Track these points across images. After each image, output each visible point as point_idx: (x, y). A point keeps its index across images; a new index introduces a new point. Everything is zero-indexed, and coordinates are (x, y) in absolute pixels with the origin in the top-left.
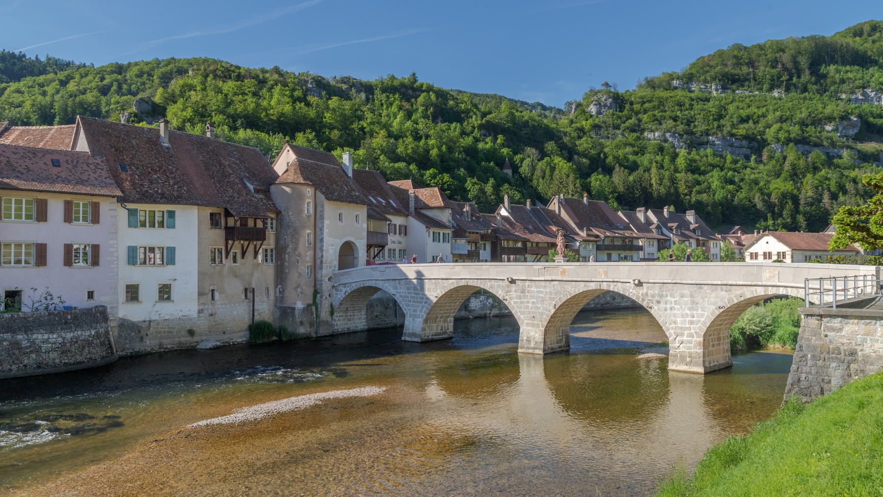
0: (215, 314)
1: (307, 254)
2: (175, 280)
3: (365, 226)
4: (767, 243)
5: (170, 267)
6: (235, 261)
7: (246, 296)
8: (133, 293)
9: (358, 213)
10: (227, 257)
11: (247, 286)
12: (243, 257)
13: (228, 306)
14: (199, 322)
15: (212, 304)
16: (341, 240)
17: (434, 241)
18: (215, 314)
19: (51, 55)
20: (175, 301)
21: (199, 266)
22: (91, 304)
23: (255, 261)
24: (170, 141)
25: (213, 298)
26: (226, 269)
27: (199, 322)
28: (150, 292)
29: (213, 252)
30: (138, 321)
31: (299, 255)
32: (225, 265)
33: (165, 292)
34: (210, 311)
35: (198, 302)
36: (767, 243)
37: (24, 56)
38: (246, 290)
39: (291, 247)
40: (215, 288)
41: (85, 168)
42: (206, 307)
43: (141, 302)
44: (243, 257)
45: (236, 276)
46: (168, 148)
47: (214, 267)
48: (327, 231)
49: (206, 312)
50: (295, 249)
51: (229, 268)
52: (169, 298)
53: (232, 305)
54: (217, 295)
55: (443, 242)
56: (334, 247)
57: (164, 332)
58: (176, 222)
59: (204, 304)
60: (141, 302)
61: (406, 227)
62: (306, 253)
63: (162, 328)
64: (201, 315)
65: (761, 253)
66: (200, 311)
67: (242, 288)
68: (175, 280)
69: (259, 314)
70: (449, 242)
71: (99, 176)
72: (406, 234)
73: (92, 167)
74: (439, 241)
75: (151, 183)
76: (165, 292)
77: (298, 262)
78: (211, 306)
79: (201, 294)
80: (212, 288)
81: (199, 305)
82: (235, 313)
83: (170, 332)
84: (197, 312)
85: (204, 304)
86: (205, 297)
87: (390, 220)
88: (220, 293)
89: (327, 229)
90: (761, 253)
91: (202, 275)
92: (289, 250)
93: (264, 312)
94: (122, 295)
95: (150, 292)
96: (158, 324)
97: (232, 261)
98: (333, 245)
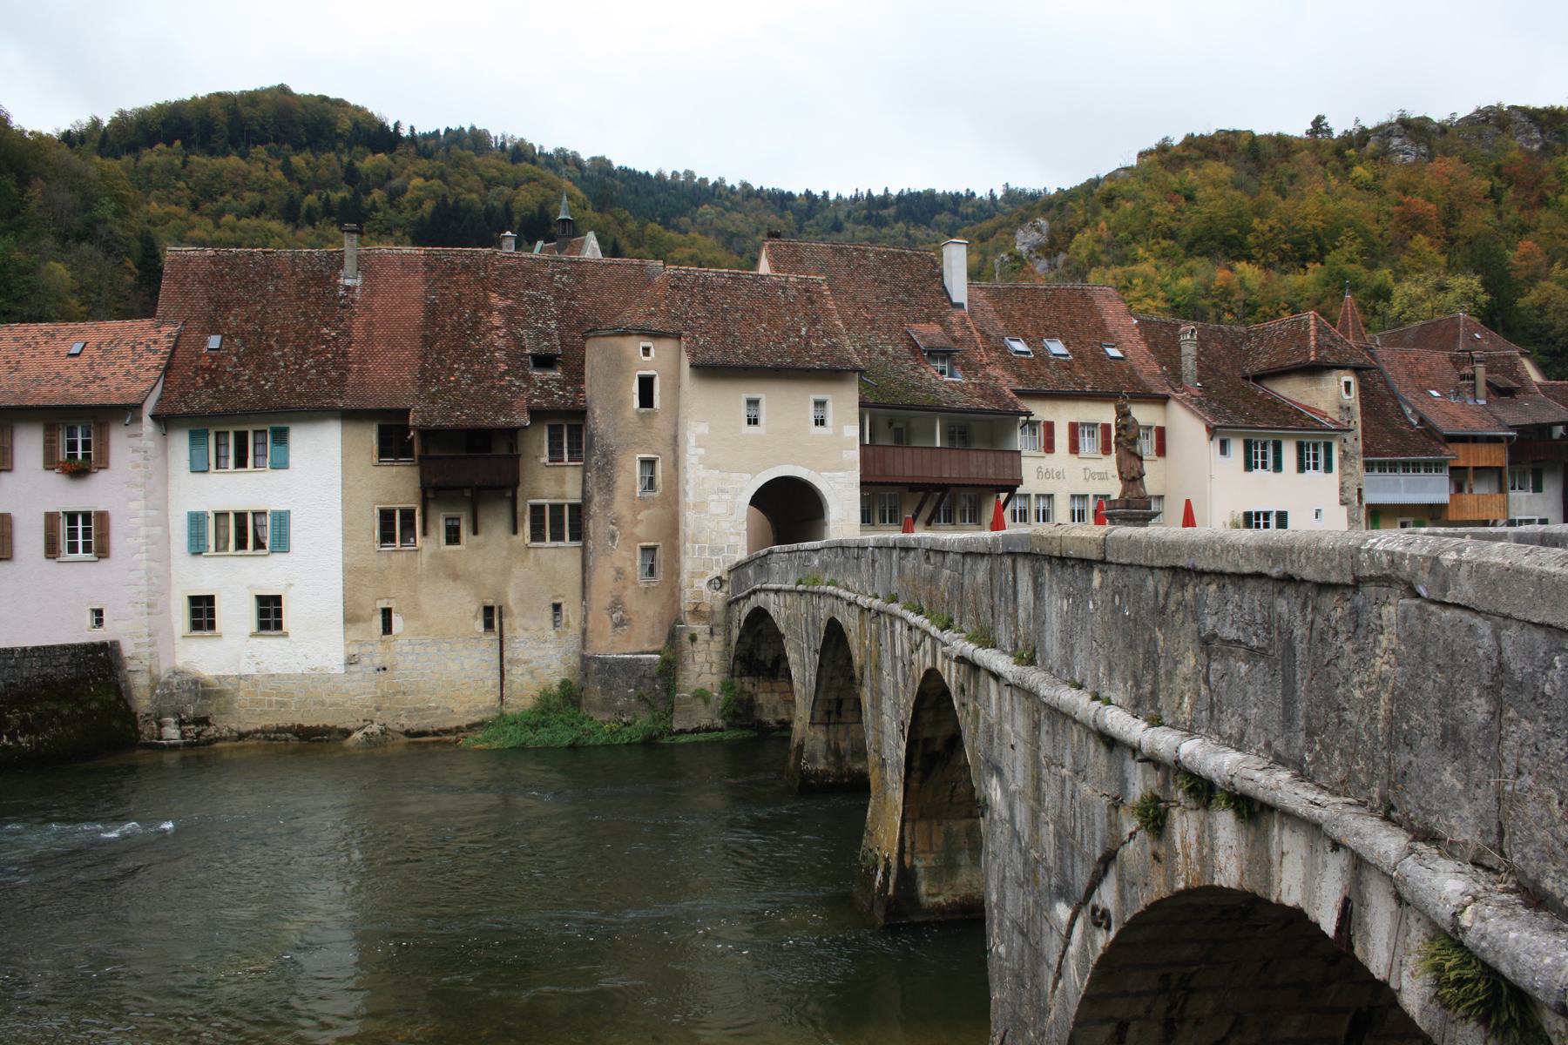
0: (394, 667)
1: (639, 517)
3: (852, 431)
5: (277, 558)
6: (453, 536)
7: (489, 625)
8: (202, 612)
9: (820, 397)
10: (425, 533)
11: (490, 602)
12: (475, 532)
13: (432, 650)
14: (348, 685)
15: (383, 642)
17: (1249, 466)
18: (394, 667)
19: (1012, 186)
21: (345, 554)
22: (98, 636)
23: (515, 538)
25: (387, 628)
26: (423, 559)
27: (348, 685)
28: (235, 613)
29: (386, 516)
30: (218, 678)
31: (615, 521)
33: (270, 612)
34: (378, 661)
35: (345, 639)
37: (973, 194)
38: (488, 611)
39: (597, 499)
40: (392, 605)
44: (475, 532)
45: (455, 577)
48: (701, 451)
49: (366, 661)
50: (607, 505)
51: (433, 556)
53: (446, 646)
54: (397, 622)
55: (1302, 468)
56: (726, 497)
57: (270, 704)
58: (292, 453)
59: (360, 643)
61: (1161, 433)
62: (635, 515)
63: (264, 694)
64: (353, 668)
66: (351, 661)
69: (531, 673)
70: (1328, 469)
74: (1278, 467)
76: (270, 612)
77: (613, 537)
78: (379, 648)
79: (350, 619)
81: (347, 646)
82: (454, 666)
83: (283, 704)
85: (360, 643)
86: (361, 626)
87: (1029, 414)
88: (406, 618)
89: (698, 446)
91: (353, 575)
93: (548, 666)
94: (181, 616)
95: (235, 613)
96: (255, 684)
97: (443, 540)
98: (723, 491)
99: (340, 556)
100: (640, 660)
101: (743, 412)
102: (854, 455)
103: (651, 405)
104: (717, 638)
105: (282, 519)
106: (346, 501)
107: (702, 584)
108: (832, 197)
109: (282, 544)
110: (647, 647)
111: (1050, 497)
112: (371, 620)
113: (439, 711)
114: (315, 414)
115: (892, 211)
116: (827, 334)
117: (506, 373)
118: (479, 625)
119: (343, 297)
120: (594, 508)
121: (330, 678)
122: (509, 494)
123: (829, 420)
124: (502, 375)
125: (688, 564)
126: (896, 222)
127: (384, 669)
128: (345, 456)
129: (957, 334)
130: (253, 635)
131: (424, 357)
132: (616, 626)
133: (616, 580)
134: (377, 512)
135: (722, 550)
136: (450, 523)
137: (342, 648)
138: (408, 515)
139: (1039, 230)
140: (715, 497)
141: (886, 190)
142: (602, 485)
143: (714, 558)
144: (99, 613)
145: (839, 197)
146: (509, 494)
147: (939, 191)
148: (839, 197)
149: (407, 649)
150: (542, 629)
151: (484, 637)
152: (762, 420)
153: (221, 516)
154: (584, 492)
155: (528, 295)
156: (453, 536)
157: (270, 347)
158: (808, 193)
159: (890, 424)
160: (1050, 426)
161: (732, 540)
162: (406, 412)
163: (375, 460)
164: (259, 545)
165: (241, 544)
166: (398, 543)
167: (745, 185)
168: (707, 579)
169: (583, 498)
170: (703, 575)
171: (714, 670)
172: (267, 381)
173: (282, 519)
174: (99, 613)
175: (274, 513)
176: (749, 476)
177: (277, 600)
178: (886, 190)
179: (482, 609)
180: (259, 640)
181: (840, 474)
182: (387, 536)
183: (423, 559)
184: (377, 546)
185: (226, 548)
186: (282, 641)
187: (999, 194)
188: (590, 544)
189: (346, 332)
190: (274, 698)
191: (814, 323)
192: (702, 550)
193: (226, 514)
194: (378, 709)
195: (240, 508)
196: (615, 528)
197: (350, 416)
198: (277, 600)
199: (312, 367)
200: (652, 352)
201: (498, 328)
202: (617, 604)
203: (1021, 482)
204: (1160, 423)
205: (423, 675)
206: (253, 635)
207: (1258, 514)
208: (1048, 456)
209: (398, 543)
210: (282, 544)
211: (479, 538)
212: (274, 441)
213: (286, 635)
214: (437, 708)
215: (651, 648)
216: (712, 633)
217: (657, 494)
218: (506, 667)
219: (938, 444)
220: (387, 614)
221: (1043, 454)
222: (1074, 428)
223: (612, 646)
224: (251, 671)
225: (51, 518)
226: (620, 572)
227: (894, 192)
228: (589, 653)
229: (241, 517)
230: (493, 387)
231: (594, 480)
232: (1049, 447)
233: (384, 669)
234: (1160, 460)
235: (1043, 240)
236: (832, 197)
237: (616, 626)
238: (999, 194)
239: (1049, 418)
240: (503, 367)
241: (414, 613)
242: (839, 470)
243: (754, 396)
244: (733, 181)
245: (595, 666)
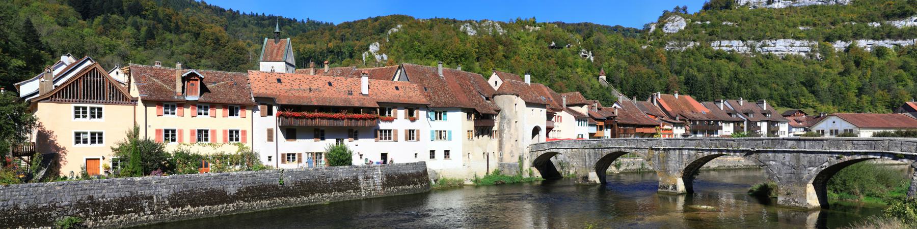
4: (834, 122)
8: (432, 153)
22: (416, 160)
24: (443, 74)
28: (440, 154)
33: (447, 153)
36: (834, 122)
37: (296, 20)
38: (484, 153)
39: (507, 130)
41: (410, 90)
45: (479, 146)
46: (443, 78)
61: (561, 117)
65: (827, 130)
71: (417, 94)
72: (561, 122)
73: (413, 90)
75: (438, 96)
76: (447, 153)
79: (464, 156)
90: (827, 130)
92: (505, 132)
95: (440, 154)
108: (241, 13)
114: (454, 109)
115: (267, 22)
126: (269, 27)
139: (376, 46)
141: (263, 14)
144: (416, 154)
145: (244, 14)
147: (284, 17)
148: (244, 14)
158: (231, 10)
165: (441, 138)
173: (450, 132)
174: (416, 154)
175: (448, 131)
178: (263, 14)
182: (469, 139)
188: (504, 139)
195: (441, 130)
197: (463, 110)
202: (511, 152)
212: (444, 114)
213: (451, 159)
223: (508, 159)
225: (406, 130)
227: (267, 15)
235: (378, 49)
238: (305, 21)
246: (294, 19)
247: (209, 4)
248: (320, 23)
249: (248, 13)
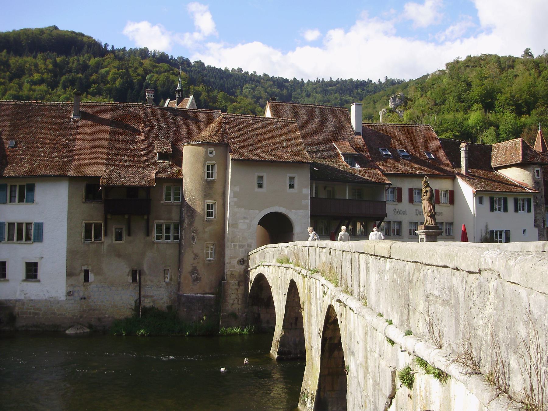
1: (206, 230)
2: (42, 258)
3: (307, 191)
5: (37, 245)
6: (119, 237)
7: (134, 280)
9: (292, 175)
10: (106, 234)
11: (135, 268)
15: (84, 286)
16: (260, 212)
19: (389, 78)
20: (41, 280)
21: (68, 243)
23: (148, 238)
25: (86, 279)
26: (105, 247)
31: (195, 231)
32: (103, 243)
34: (81, 294)
35: (67, 284)
37: (371, 81)
39: (186, 221)
40: (90, 268)
42: (76, 289)
43: (8, 281)
44: (129, 234)
45: (119, 256)
47: (88, 244)
49: (76, 294)
50: (191, 224)
52: (35, 276)
54: (91, 277)
56: (247, 221)
57: (30, 313)
60: (8, 281)
64: (69, 298)
66: (69, 294)
67: (127, 270)
68: (42, 258)
69: (154, 301)
74: (506, 210)
77: (193, 239)
78: (82, 288)
79: (70, 274)
80: (85, 268)
81: (67, 287)
84: (65, 295)
88: (96, 274)
91: (71, 254)
93: (162, 299)
96: (23, 304)
97: (114, 238)
98: (245, 218)
99: (66, 245)
100: (204, 297)
101: (255, 182)
102: (307, 202)
103: (212, 177)
104: (241, 287)
105: (39, 227)
106: (70, 219)
107: (235, 262)
109: (39, 238)
110: (207, 291)
111: (400, 223)
112: (79, 275)
113: (110, 319)
116: (296, 146)
117: (147, 161)
118: (130, 279)
119: (72, 124)
120: (185, 225)
121: (58, 302)
122: (146, 217)
123: (296, 186)
124: (145, 162)
125: (228, 253)
126: (335, 93)
127: (85, 298)
128: (70, 197)
129: (358, 147)
130: (23, 281)
131: (108, 153)
132: (194, 281)
133: (194, 259)
134: (83, 224)
135: (244, 246)
136: (117, 230)
137: (65, 288)
138: (98, 227)
140: (242, 221)
142: (189, 214)
143: (241, 249)
145: (309, 81)
146: (146, 217)
147: (355, 79)
148: (309, 81)
149: (96, 289)
150: (159, 281)
151: (132, 285)
152: (265, 185)
153: (11, 225)
154: (180, 217)
155: (157, 125)
156: (119, 237)
157: (38, 147)
158: (295, 79)
159: (325, 189)
160: (400, 190)
161: (249, 241)
162: (99, 178)
163: (84, 200)
164: (28, 238)
165: (20, 238)
166: (93, 239)
167: (266, 75)
168: (237, 259)
169: (180, 221)
170: (235, 258)
171: (240, 303)
172: (36, 162)
173: (39, 227)
176: (258, 211)
177: (35, 264)
179: (131, 271)
180: (25, 283)
181: (301, 211)
182: (88, 236)
183: (105, 247)
184: (83, 240)
185: (13, 240)
186: (37, 284)
187: (383, 81)
188: (183, 242)
189: (73, 141)
190: (32, 311)
191: (289, 141)
192: (235, 246)
193: (13, 224)
194: (81, 317)
196: (195, 234)
197: (73, 180)
198: (35, 264)
199: (56, 157)
200: (214, 152)
201: (143, 140)
202: (194, 270)
203: (386, 216)
204: (451, 189)
205: (103, 302)
206: (23, 281)
207: (496, 232)
208: (399, 204)
209: (93, 239)
210: (39, 238)
211: (131, 238)
213: (39, 281)
214: (109, 317)
215: (210, 292)
216: (239, 285)
217: (215, 219)
218: (142, 299)
219: (347, 198)
220: (86, 272)
221: (397, 203)
222: (411, 191)
224: (22, 297)
226: (196, 255)
228: (181, 293)
229: (20, 225)
230: (140, 167)
231: (185, 212)
232: (400, 200)
233: (85, 298)
234: (451, 206)
236: (305, 81)
237: (194, 281)
238: (383, 81)
239: (399, 186)
240: (145, 159)
241: (98, 273)
242: (300, 210)
243: (261, 174)
244: (260, 73)
245: (183, 299)
246: (369, 79)
247: (271, 76)
248: (402, 81)
249: (313, 80)
